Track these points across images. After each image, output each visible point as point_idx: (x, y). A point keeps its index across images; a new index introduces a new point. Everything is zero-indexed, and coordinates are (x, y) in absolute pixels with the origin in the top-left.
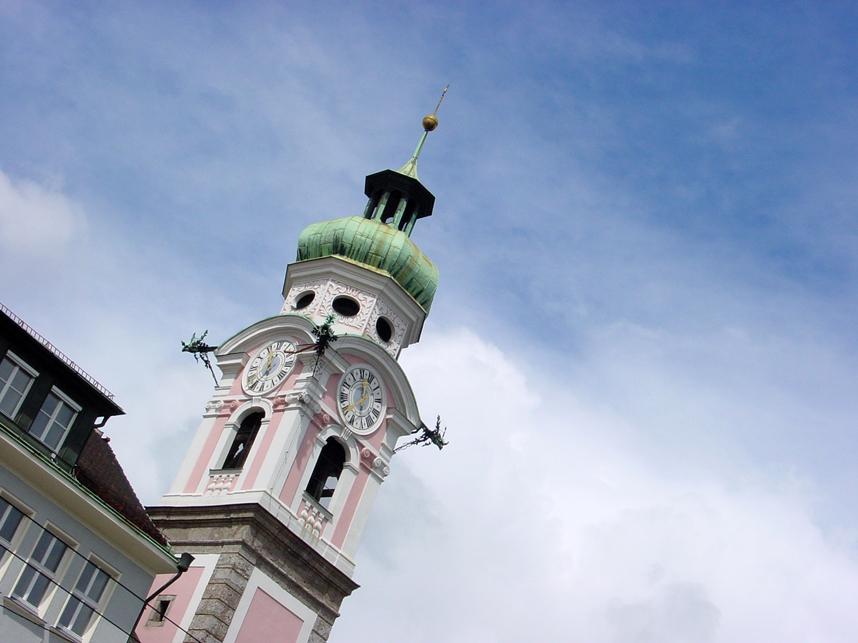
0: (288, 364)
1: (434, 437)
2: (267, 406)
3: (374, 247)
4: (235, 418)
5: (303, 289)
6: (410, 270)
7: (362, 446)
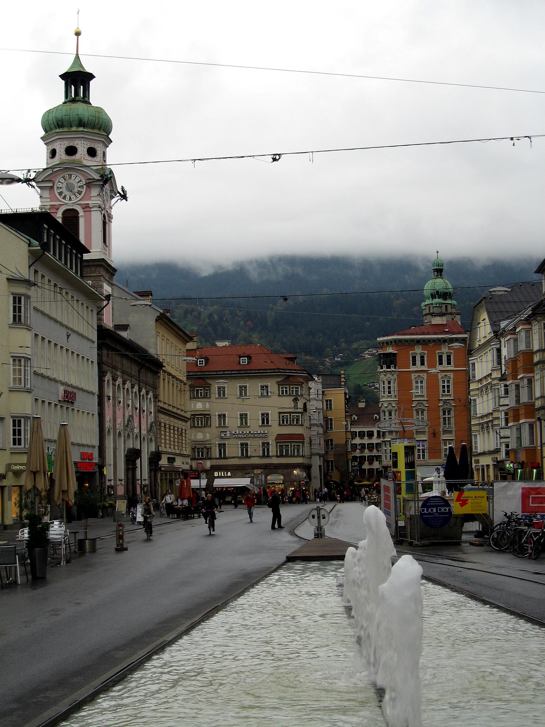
0: (80, 187)
1: (124, 197)
3: (97, 121)
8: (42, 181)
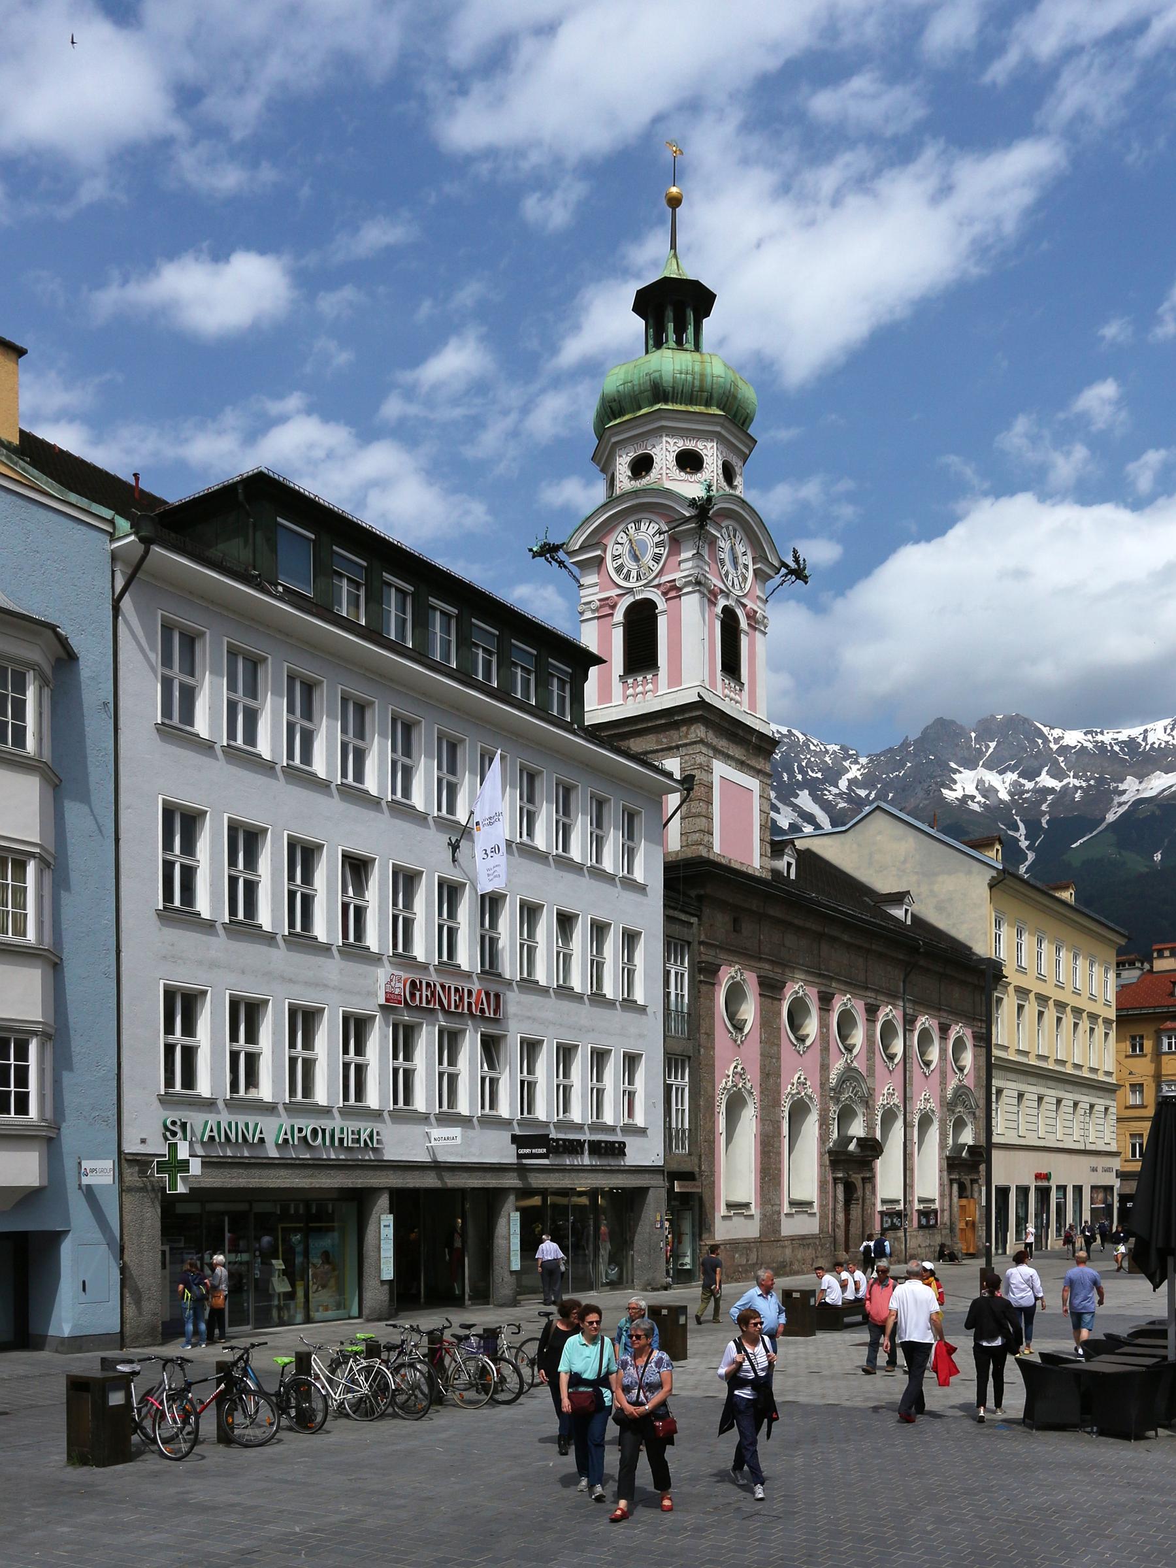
0: (657, 545)
2: (656, 596)
3: (697, 383)
4: (619, 616)
5: (632, 455)
6: (735, 397)
7: (744, 606)
8: (581, 548)
